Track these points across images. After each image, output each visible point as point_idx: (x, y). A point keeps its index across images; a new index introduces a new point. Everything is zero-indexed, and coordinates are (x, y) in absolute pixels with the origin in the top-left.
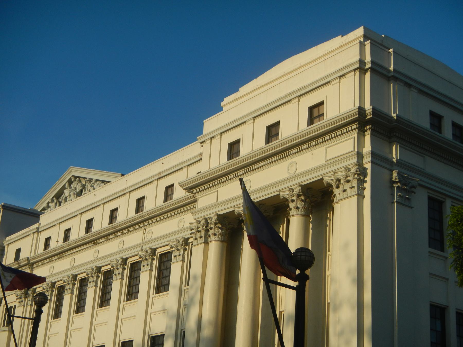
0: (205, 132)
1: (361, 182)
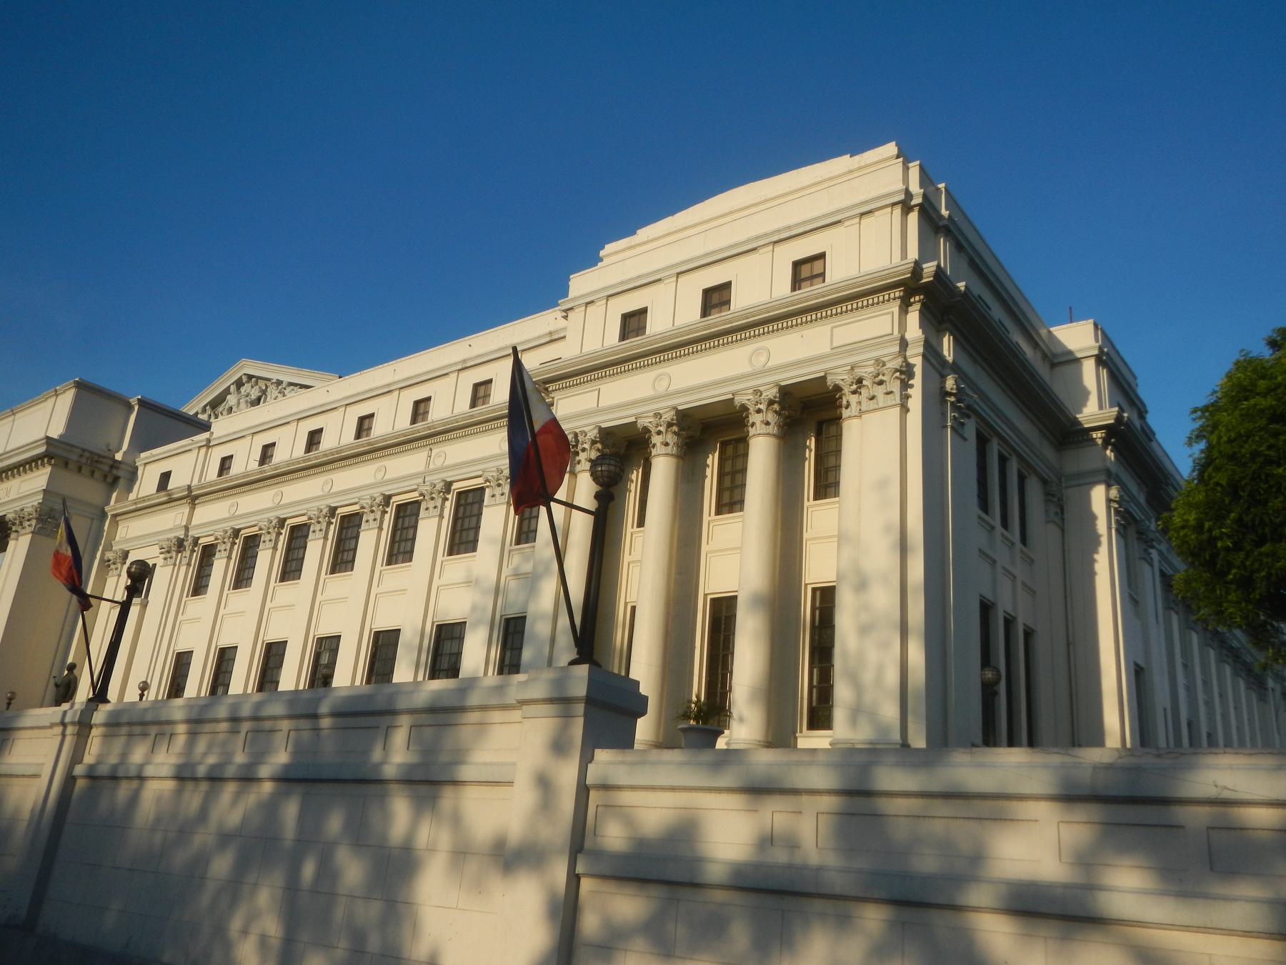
0: (572, 294)
1: (905, 385)
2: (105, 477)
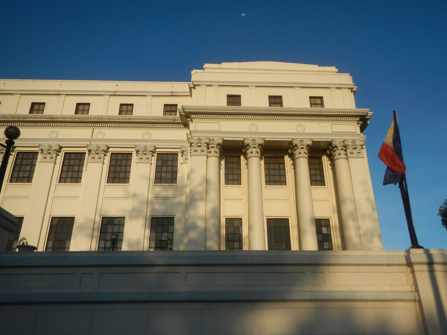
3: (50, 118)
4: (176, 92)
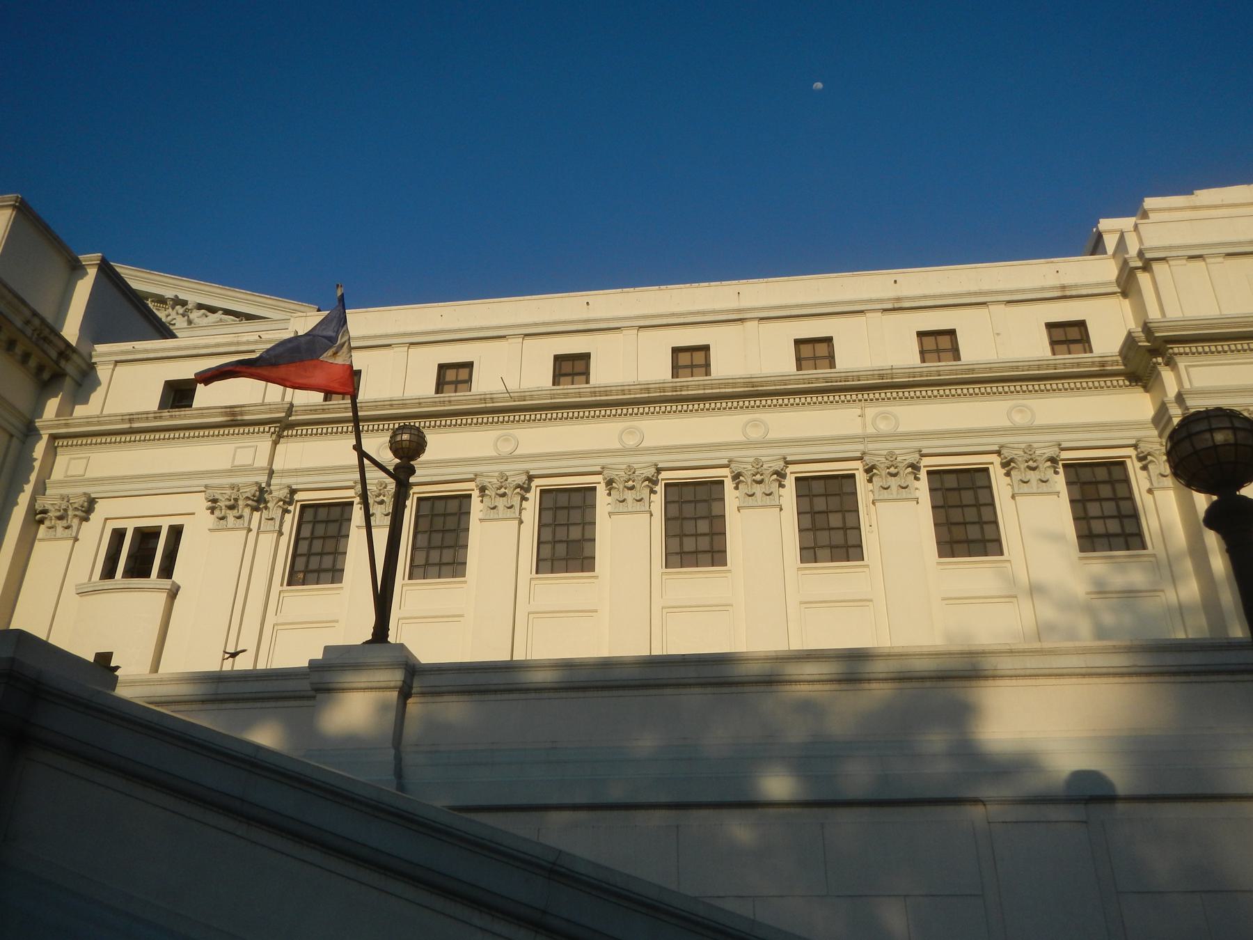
2: (40, 369)
3: (746, 384)
4: (1076, 286)
